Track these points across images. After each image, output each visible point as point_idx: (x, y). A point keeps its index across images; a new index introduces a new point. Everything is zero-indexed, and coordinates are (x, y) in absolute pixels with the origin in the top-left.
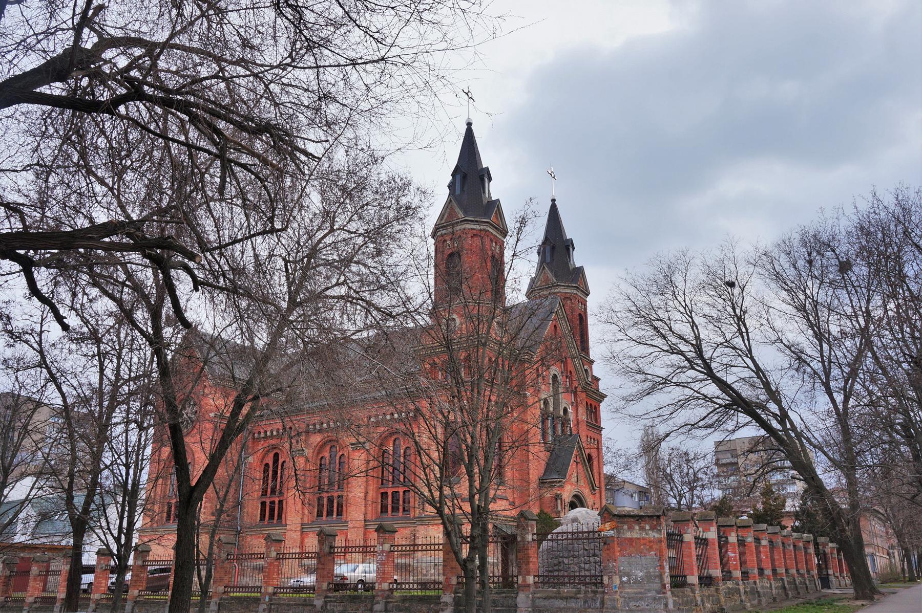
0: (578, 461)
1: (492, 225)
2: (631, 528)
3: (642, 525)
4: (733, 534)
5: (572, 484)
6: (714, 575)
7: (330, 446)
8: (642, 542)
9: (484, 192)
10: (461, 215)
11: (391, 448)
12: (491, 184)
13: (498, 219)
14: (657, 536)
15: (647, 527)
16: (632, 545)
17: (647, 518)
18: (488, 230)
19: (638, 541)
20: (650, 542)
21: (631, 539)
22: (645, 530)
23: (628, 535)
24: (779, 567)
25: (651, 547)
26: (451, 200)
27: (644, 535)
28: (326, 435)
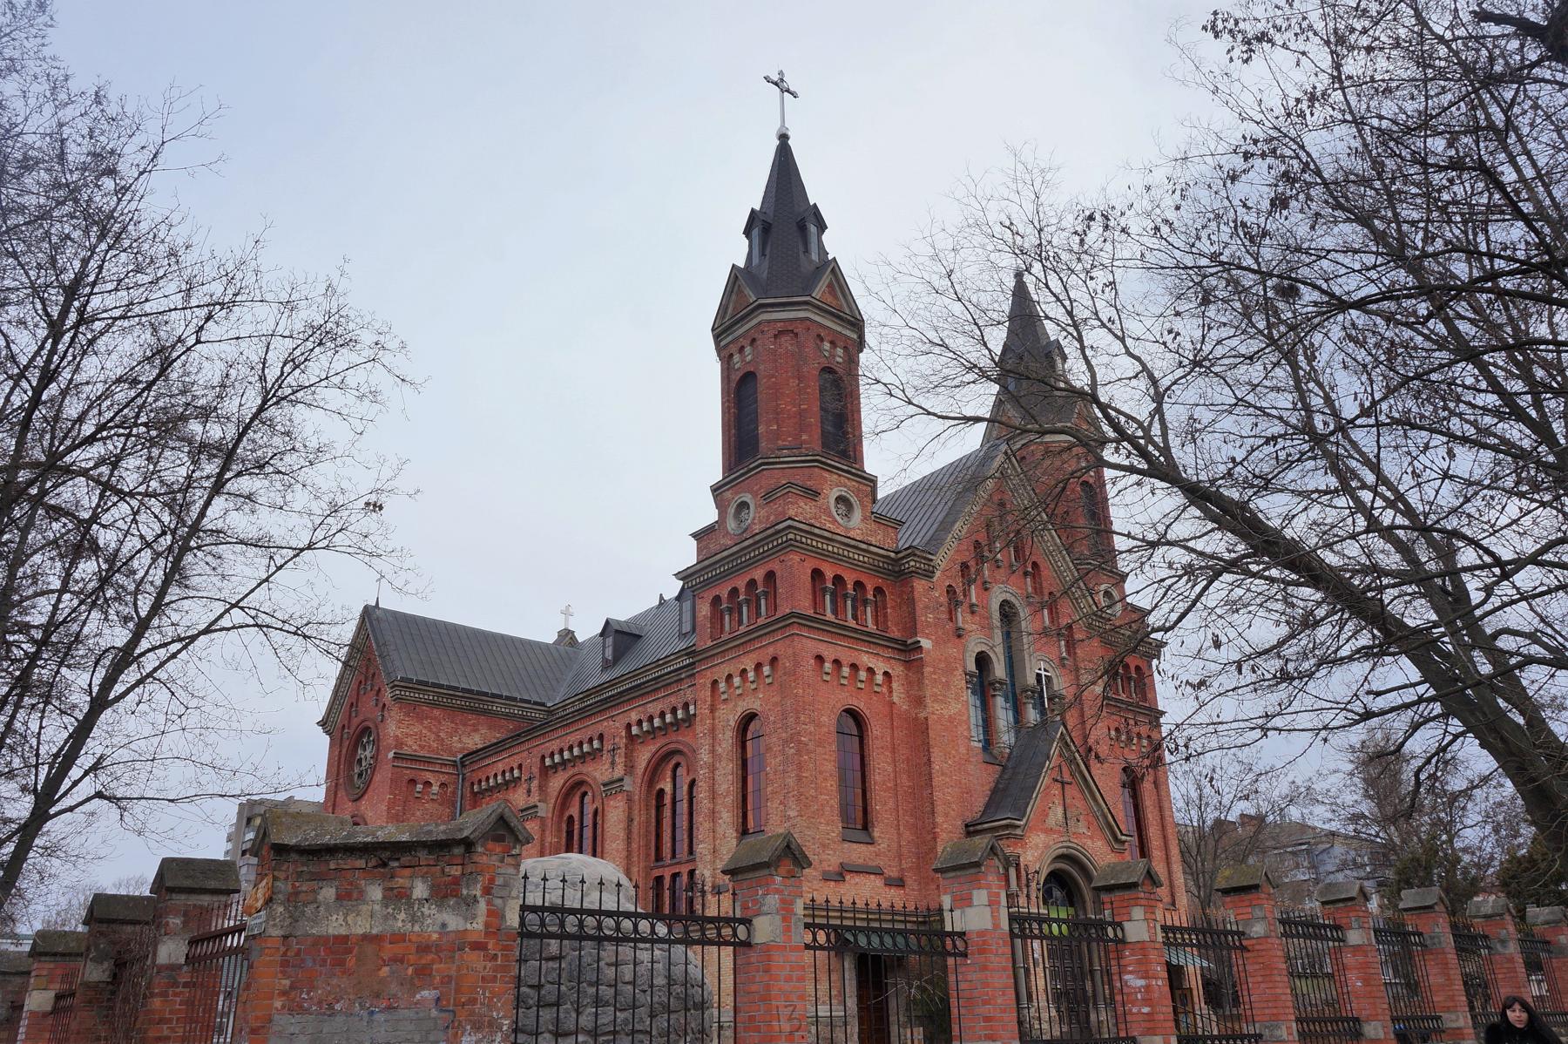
0: (1067, 778)
2: (349, 897)
3: (400, 881)
4: (1138, 913)
5: (1048, 831)
7: (579, 794)
8: (388, 950)
9: (807, 251)
11: (668, 788)
12: (825, 237)
13: (835, 297)
14: (454, 922)
15: (420, 890)
16: (341, 963)
17: (423, 855)
19: (370, 949)
20: (424, 948)
21: (343, 939)
22: (410, 905)
23: (335, 925)
24: (1448, 1009)
25: (423, 972)
27: (401, 922)
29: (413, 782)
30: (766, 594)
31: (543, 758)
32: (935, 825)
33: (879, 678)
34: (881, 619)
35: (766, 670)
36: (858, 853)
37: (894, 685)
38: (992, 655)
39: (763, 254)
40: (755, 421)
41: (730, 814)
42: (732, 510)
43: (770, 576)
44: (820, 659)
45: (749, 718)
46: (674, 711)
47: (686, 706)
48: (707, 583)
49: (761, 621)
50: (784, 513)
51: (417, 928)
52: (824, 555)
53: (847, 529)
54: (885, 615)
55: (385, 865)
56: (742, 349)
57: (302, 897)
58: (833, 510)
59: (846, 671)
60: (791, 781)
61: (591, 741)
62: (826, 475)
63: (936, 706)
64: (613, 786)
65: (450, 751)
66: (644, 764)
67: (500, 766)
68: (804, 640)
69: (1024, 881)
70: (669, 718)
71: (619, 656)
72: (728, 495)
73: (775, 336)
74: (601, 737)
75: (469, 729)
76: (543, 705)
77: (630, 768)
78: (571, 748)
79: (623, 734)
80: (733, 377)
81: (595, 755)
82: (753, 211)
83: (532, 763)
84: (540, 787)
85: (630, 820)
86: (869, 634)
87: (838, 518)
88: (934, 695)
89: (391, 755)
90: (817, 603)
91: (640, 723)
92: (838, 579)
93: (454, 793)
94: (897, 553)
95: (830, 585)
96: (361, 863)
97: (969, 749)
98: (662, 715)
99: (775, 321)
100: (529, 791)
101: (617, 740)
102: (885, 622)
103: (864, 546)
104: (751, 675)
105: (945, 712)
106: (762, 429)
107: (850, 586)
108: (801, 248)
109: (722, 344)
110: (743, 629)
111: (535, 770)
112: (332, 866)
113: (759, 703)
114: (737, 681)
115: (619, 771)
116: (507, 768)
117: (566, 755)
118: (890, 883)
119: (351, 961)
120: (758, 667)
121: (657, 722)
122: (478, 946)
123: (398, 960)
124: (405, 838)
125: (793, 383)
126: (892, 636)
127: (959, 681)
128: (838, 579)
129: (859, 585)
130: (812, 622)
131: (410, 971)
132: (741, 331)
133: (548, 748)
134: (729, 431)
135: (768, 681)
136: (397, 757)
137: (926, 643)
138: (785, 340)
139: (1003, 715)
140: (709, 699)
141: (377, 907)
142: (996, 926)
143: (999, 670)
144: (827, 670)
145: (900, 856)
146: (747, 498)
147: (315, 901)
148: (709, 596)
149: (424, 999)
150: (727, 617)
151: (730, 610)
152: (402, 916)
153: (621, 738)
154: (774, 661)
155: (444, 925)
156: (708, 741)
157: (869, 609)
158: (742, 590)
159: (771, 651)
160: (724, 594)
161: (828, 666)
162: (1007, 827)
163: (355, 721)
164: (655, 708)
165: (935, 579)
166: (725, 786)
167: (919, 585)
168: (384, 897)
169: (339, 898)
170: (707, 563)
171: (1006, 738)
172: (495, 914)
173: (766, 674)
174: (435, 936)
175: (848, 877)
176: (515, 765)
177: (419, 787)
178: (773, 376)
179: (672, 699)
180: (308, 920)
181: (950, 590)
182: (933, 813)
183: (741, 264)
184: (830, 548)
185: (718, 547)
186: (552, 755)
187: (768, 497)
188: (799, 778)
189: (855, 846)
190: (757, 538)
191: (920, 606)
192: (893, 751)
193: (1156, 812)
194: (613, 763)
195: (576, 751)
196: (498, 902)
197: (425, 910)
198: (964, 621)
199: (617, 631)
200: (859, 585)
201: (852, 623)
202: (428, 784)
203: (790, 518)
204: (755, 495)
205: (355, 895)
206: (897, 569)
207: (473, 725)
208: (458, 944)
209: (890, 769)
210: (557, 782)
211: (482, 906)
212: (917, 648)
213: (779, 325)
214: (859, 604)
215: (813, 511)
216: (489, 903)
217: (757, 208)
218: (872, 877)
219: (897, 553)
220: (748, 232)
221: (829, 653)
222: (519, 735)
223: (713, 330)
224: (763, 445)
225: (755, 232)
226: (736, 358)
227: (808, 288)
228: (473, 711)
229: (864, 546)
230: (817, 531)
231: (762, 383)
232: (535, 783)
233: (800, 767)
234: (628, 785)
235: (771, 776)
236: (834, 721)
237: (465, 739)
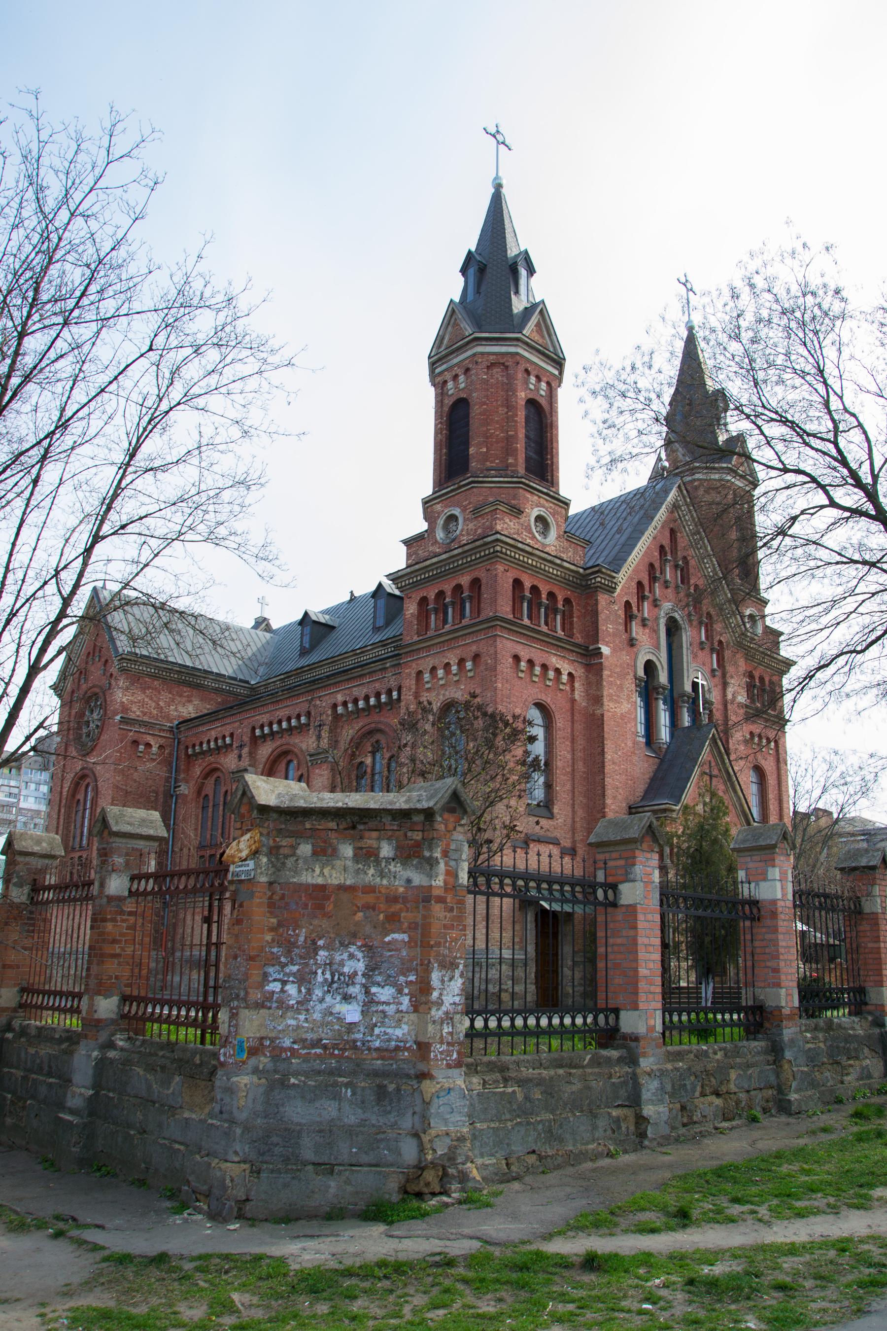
0: (715, 772)
1: (527, 344)
7: (285, 761)
8: (364, 899)
10: (468, 329)
12: (534, 280)
13: (543, 337)
14: (418, 879)
15: (386, 850)
16: (321, 907)
18: (517, 354)
19: (345, 897)
20: (393, 899)
21: (323, 888)
22: (378, 861)
23: (313, 877)
26: (453, 311)
27: (370, 875)
29: (136, 743)
30: (470, 598)
31: (254, 729)
32: (604, 806)
33: (565, 678)
34: (567, 626)
35: (469, 665)
37: (577, 685)
38: (657, 663)
39: (478, 292)
40: (466, 444)
42: (441, 522)
43: (476, 583)
44: (517, 658)
46: (378, 695)
47: (389, 692)
49: (465, 622)
50: (491, 528)
51: (385, 882)
52: (524, 566)
53: (544, 545)
54: (571, 623)
55: (354, 827)
56: (455, 377)
57: (282, 851)
59: (538, 670)
61: (298, 717)
62: (528, 495)
63: (612, 705)
65: (168, 717)
67: (213, 734)
68: (505, 641)
70: (372, 701)
71: (315, 643)
72: (438, 507)
73: (488, 367)
75: (184, 700)
76: (247, 682)
78: (280, 722)
79: (329, 712)
80: (446, 401)
81: (302, 729)
82: (470, 252)
83: (243, 731)
86: (559, 639)
87: (537, 535)
88: (610, 695)
89: (118, 718)
90: (516, 608)
92: (535, 589)
93: (171, 754)
94: (585, 569)
95: (527, 594)
96: (333, 825)
97: (635, 743)
98: (367, 698)
99: (489, 354)
100: (240, 757)
102: (572, 629)
103: (558, 561)
104: (454, 668)
105: (618, 710)
106: (472, 450)
107: (544, 596)
109: (437, 371)
111: (246, 739)
112: (308, 826)
114: (440, 673)
116: (220, 735)
117: (275, 727)
119: (329, 907)
121: (361, 704)
122: (441, 900)
123: (367, 907)
125: (502, 410)
126: (577, 641)
127: (630, 685)
128: (535, 589)
129: (551, 595)
130: (512, 626)
131: (381, 916)
132: (456, 361)
133: (258, 720)
134: (441, 450)
136: (124, 721)
137: (605, 650)
138: (497, 371)
139: (663, 718)
140: (413, 687)
141: (349, 863)
143: (663, 678)
144: (523, 668)
145: (573, 830)
146: (457, 512)
147: (294, 854)
148: (417, 596)
149: (394, 941)
150: (433, 617)
151: (436, 610)
152: (372, 871)
153: (327, 716)
154: (476, 657)
155: (409, 881)
157: (559, 617)
158: (449, 593)
159: (474, 648)
160: (432, 596)
161: (523, 665)
162: (665, 810)
163: (84, 687)
164: (359, 692)
165: (616, 594)
167: (603, 599)
168: (355, 855)
169: (315, 853)
170: (412, 569)
171: (664, 734)
172: (452, 874)
173: (469, 668)
174: (401, 890)
175: (531, 845)
176: (227, 734)
177: (141, 748)
178: (485, 404)
179: (377, 685)
180: (290, 870)
181: (628, 605)
182: (604, 795)
183: (457, 299)
185: (426, 554)
186: (262, 727)
187: (477, 512)
190: (466, 548)
191: (602, 617)
192: (573, 741)
193: (776, 803)
194: (319, 737)
195: (284, 725)
196: (452, 863)
197: (392, 867)
198: (637, 633)
199: (314, 622)
200: (551, 595)
201: (544, 628)
202: (148, 745)
204: (464, 510)
205: (329, 851)
206: (584, 583)
207: (188, 696)
209: (569, 756)
211: (442, 866)
212: (599, 654)
213: (491, 357)
215: (517, 527)
216: (446, 864)
217: (473, 249)
218: (551, 846)
219: (585, 569)
220: (464, 271)
221: (525, 653)
222: (231, 708)
223: (429, 357)
224: (473, 464)
225: (471, 271)
226: (450, 385)
227: (520, 329)
228: (190, 685)
229: (558, 561)
230: (520, 545)
231: (475, 411)
232: (245, 751)
237: (180, 709)
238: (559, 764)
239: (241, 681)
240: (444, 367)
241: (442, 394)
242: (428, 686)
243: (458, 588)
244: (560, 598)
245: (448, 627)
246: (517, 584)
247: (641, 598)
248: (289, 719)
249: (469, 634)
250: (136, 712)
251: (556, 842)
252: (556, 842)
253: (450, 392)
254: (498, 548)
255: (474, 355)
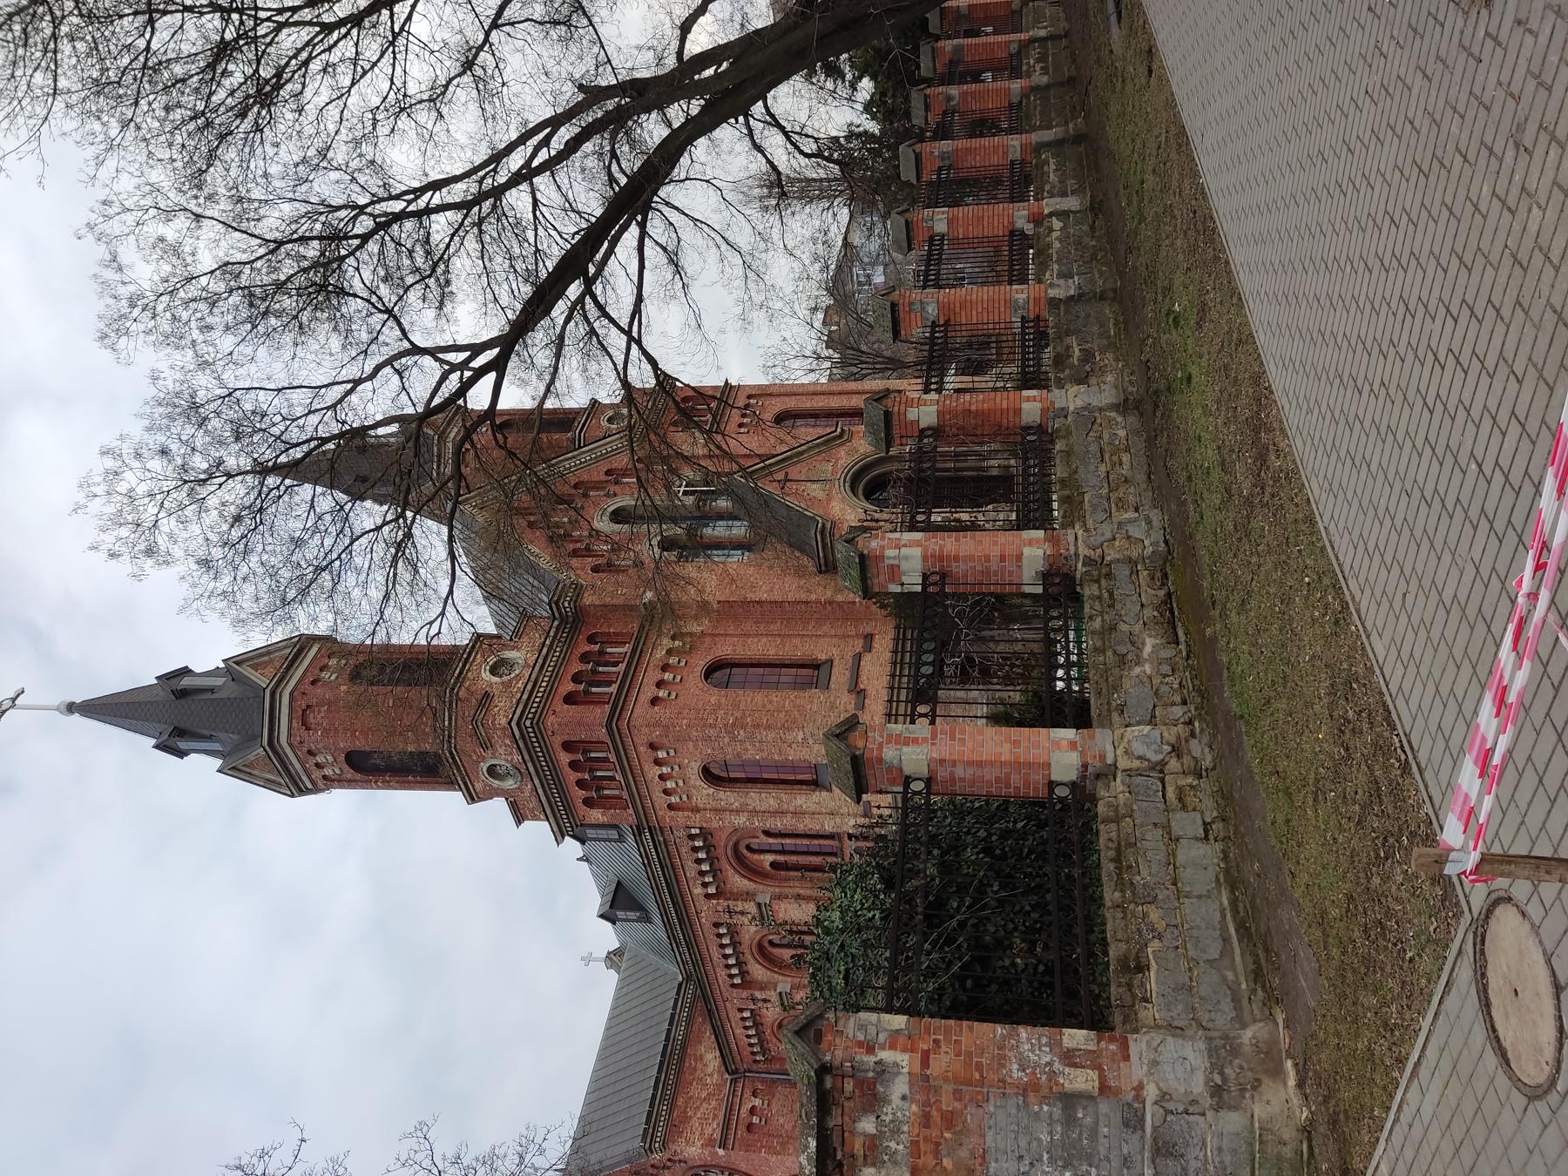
4: (912, 414)
5: (829, 498)
6: (1040, 566)
7: (770, 949)
9: (212, 690)
11: (770, 858)
12: (198, 669)
13: (271, 661)
14: (900, 1087)
15: (867, 1125)
18: (291, 694)
24: (1005, 153)
25: (950, 1120)
27: (898, 1146)
28: (749, 957)
29: (750, 1127)
30: (585, 752)
31: (733, 986)
32: (818, 602)
34: (620, 639)
35: (661, 754)
36: (840, 676)
39: (210, 738)
41: (798, 797)
42: (496, 783)
43: (568, 746)
44: (655, 701)
45: (708, 774)
46: (695, 849)
47: (692, 837)
48: (569, 809)
49: (612, 758)
50: (504, 729)
51: (905, 1128)
52: (550, 691)
53: (526, 665)
55: (840, 1165)
56: (318, 765)
58: (505, 678)
59: (668, 676)
60: (771, 736)
61: (720, 936)
64: (763, 916)
65: (719, 1086)
66: (746, 882)
67: (739, 1031)
68: (635, 715)
69: (874, 524)
70: (702, 855)
71: (636, 905)
72: (479, 786)
73: (308, 729)
74: (717, 925)
75: (699, 1066)
76: (680, 985)
77: (748, 896)
78: (726, 957)
79: (715, 902)
81: (733, 932)
82: (157, 747)
83: (736, 998)
84: (762, 989)
85: (798, 897)
86: (634, 650)
89: (721, 1152)
90: (598, 701)
91: (705, 885)
92: (576, 679)
93: (763, 1081)
94: (555, 618)
97: (748, 564)
98: (699, 861)
99: (290, 728)
101: (719, 908)
102: (622, 634)
103: (545, 650)
104: (665, 770)
108: (208, 696)
109: (310, 786)
110: (619, 777)
111: (745, 994)
113: (693, 763)
114: (670, 784)
115: (751, 908)
116: (741, 1024)
117: (732, 961)
118: (868, 648)
120: (658, 762)
121: (705, 867)
122: (925, 1062)
124: (813, 1144)
126: (636, 629)
128: (576, 679)
129: (585, 658)
130: (618, 706)
131: (947, 1135)
132: (298, 766)
133: (724, 981)
134: (409, 782)
135: (672, 753)
136: (723, 1145)
139: (718, 530)
140: (686, 813)
142: (917, 544)
145: (844, 637)
146: (484, 766)
148: (582, 809)
150: (606, 792)
151: (599, 789)
153: (718, 904)
155: (904, 1098)
156: (727, 815)
157: (609, 650)
159: (642, 749)
166: (771, 801)
167: (588, 599)
168: (874, 1165)
171: (739, 530)
173: (665, 755)
174: (914, 1108)
175: (862, 687)
176: (739, 1015)
177: (755, 1120)
179: (684, 850)
181: (596, 569)
182: (807, 602)
183: (218, 763)
184: (544, 684)
185: (533, 799)
186: (731, 976)
187: (486, 745)
188: (768, 727)
189: (833, 679)
190: (527, 757)
192: (747, 635)
194: (742, 913)
195: (729, 951)
196: (882, 1037)
197: (888, 1118)
199: (611, 907)
200: (585, 658)
201: (622, 667)
202: (753, 1111)
203: (510, 723)
204: (484, 759)
206: (571, 620)
207: (696, 1061)
208: (923, 1082)
209: (764, 640)
210: (758, 971)
211: (885, 1055)
213: (295, 724)
214: (603, 659)
216: (883, 1048)
217: (153, 741)
219: (555, 618)
220: (181, 754)
221: (649, 691)
222: (709, 1011)
223: (292, 796)
225: (182, 745)
226: (328, 772)
228: (681, 1060)
229: (545, 650)
230: (525, 697)
231: (361, 744)
232: (758, 994)
233: (757, 726)
234: (764, 898)
235: (765, 755)
236: (716, 690)
237: (710, 1070)
238: (772, 652)
239: (678, 993)
240: (305, 778)
241: (339, 781)
242: (685, 798)
243: (574, 765)
244: (588, 648)
245: (619, 777)
246: (570, 699)
247: (589, 552)
248: (722, 946)
249: (626, 754)
250: (713, 1129)
251: (858, 658)
252: (858, 658)
253: (338, 772)
254: (528, 723)
255: (291, 745)
